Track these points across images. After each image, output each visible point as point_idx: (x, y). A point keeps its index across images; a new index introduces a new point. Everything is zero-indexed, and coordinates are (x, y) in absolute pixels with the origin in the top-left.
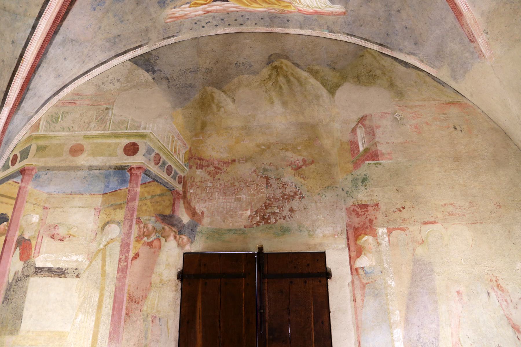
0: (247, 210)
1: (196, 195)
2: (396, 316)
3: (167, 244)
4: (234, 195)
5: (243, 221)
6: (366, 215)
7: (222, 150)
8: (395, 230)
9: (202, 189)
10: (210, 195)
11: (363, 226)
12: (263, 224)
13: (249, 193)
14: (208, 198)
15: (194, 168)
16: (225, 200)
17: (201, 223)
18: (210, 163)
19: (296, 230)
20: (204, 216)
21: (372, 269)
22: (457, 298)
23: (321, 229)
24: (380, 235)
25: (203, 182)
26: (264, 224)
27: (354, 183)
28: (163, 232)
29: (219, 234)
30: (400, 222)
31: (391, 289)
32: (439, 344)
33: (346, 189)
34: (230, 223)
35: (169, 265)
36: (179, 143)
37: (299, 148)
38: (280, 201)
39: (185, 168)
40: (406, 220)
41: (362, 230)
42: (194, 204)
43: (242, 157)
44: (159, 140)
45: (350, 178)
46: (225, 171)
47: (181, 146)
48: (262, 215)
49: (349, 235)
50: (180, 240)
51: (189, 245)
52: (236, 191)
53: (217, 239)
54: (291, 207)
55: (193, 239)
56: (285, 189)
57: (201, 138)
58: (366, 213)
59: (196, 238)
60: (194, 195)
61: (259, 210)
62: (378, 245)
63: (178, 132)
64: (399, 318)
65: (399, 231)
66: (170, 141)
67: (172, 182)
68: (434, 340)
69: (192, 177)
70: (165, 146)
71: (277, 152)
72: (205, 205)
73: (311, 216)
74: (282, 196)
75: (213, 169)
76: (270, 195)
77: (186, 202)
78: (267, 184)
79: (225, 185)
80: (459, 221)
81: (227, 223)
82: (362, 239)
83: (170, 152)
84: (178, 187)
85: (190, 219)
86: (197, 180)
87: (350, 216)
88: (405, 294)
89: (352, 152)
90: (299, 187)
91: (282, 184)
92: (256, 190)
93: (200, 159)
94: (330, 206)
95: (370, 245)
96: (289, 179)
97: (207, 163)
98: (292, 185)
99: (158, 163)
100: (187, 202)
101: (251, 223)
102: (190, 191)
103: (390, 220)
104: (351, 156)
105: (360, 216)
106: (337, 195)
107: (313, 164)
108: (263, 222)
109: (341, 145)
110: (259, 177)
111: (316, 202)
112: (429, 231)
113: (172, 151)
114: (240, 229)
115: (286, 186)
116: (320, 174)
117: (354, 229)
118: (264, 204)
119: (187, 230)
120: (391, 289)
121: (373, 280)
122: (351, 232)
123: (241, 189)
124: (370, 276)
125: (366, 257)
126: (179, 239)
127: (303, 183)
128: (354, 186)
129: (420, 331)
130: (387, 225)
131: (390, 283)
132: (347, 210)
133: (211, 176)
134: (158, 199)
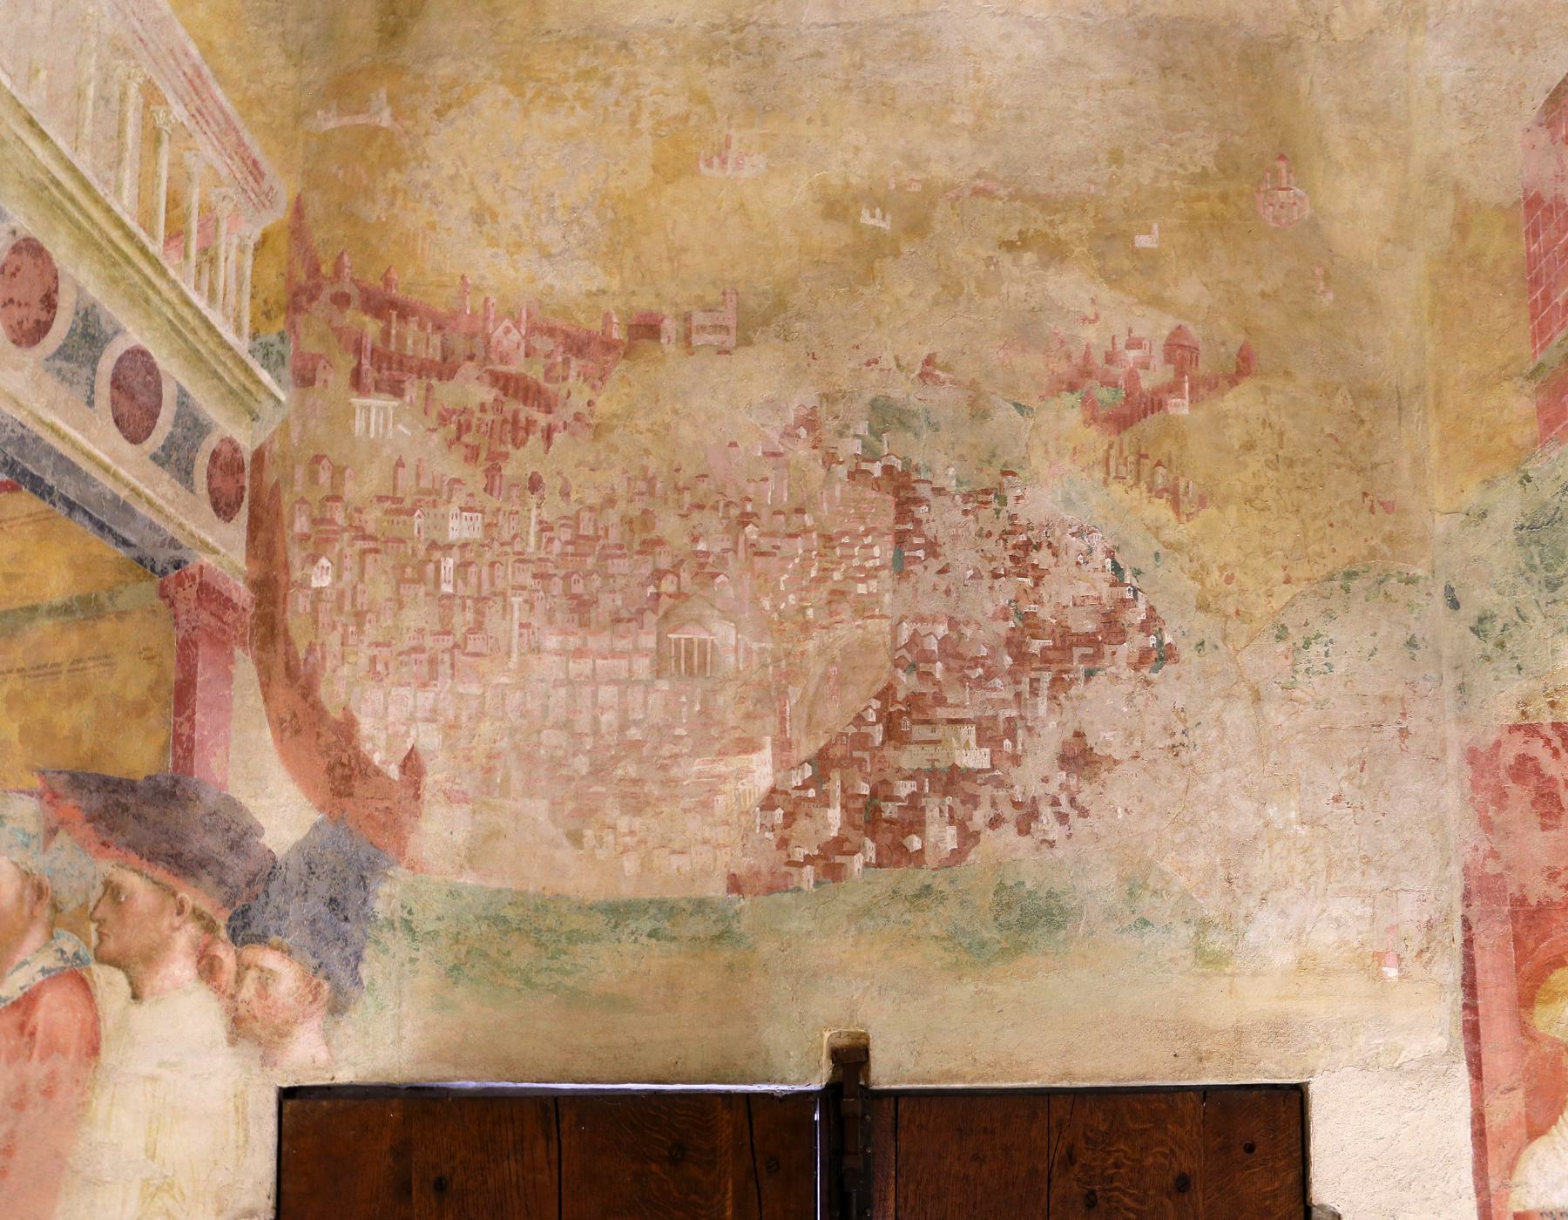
0: (748, 746)
1: (359, 616)
3: (141, 1015)
4: (651, 619)
5: (721, 835)
7: (550, 234)
9: (403, 567)
10: (470, 616)
12: (867, 865)
13: (766, 604)
14: (448, 642)
15: (336, 379)
16: (585, 666)
17: (401, 854)
18: (460, 346)
19: (1111, 915)
20: (426, 795)
23: (1283, 913)
25: (407, 504)
26: (879, 865)
27: (1534, 549)
28: (111, 917)
29: (538, 944)
33: (1480, 597)
34: (626, 850)
35: (167, 1186)
36: (206, 154)
37: (1143, 241)
38: (998, 682)
39: (265, 376)
42: (340, 688)
43: (713, 296)
44: (31, 122)
45: (1509, 506)
46: (578, 417)
47: (219, 183)
48: (865, 789)
49: (1478, 965)
50: (249, 990)
51: (315, 1022)
52: (668, 585)
53: (528, 982)
54: (1079, 735)
55: (343, 976)
56: (1038, 581)
57: (385, 119)
59: (364, 971)
60: (340, 609)
61: (838, 752)
63: (193, 50)
66: (131, 133)
67: (159, 501)
69: (318, 459)
70: (88, 173)
71: (980, 268)
72: (426, 699)
73: (1221, 804)
74: (1009, 642)
75: (487, 394)
76: (923, 629)
77: (279, 671)
78: (901, 539)
79: (577, 539)
81: (601, 854)
83: (130, 236)
84: (210, 540)
85: (318, 817)
86: (364, 484)
87: (1492, 809)
89: (1538, 294)
90: (1137, 573)
91: (1012, 541)
92: (819, 580)
93: (382, 305)
94: (1358, 728)
96: (1068, 502)
97: (436, 340)
98: (1090, 551)
99: (42, 328)
100: (291, 672)
101: (783, 855)
102: (304, 584)
104: (1526, 327)
106: (1411, 643)
107: (1247, 386)
108: (869, 844)
109: (1462, 227)
110: (841, 471)
111: (1257, 698)
113: (147, 223)
114: (701, 905)
115: (1041, 558)
116: (1291, 464)
117: (1514, 915)
118: (876, 704)
119: (297, 910)
122: (1494, 936)
123: (705, 571)
126: (239, 979)
127: (1169, 534)
128: (1535, 577)
132: (1471, 763)
133: (473, 455)
134: (61, 643)
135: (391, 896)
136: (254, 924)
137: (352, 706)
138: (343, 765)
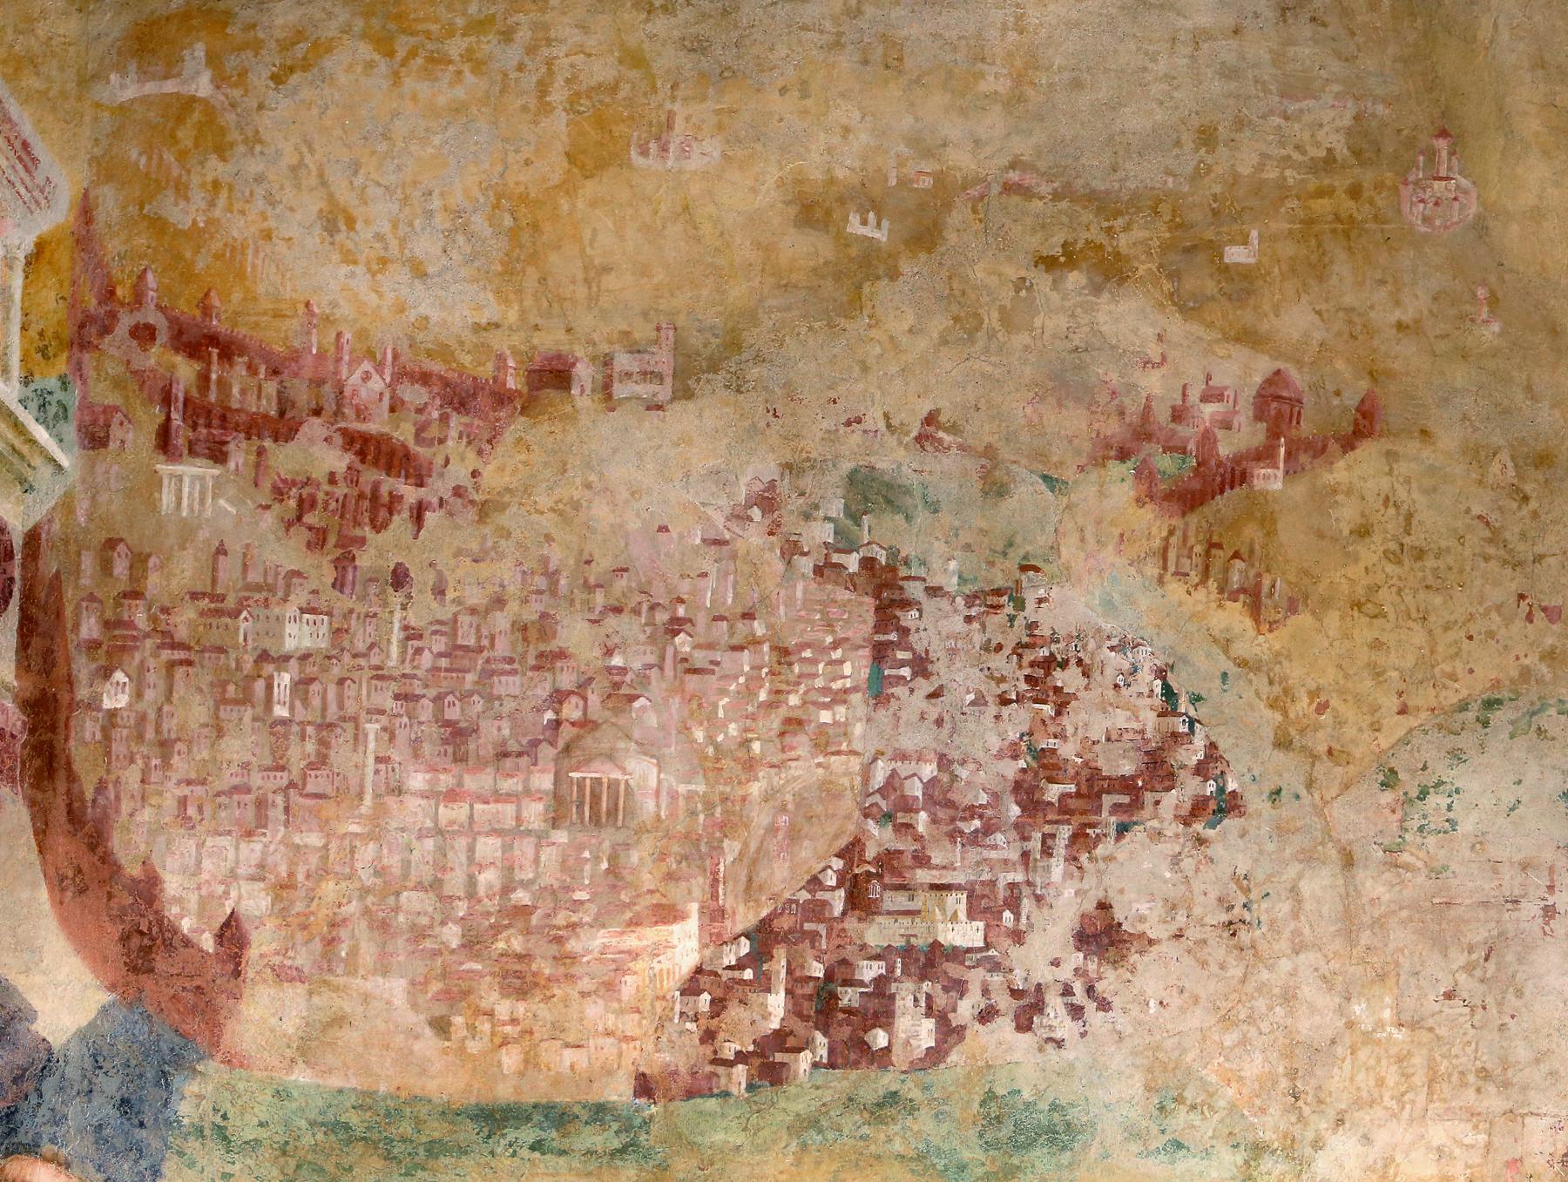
17: (216, 1045)
85: (106, 997)
135: (200, 1097)
136: (22, 1130)
137: (155, 860)
138: (142, 933)
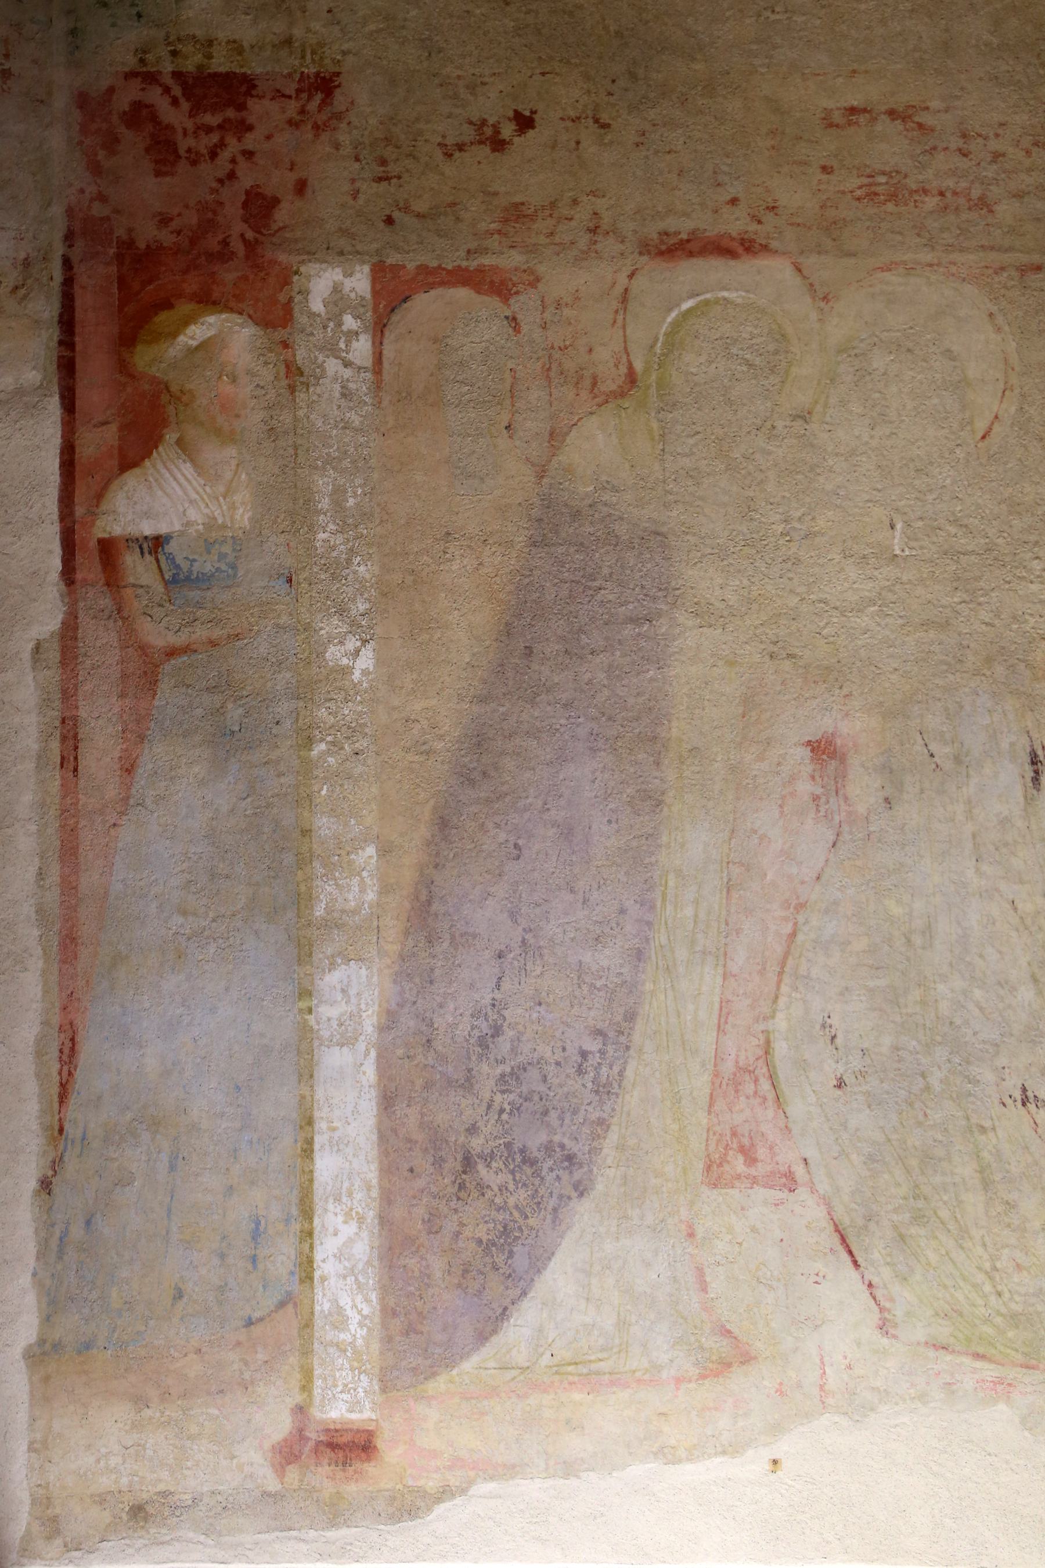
2: (355, 881)
6: (225, 155)
8: (429, 287)
11: (193, 242)
21: (222, 556)
22: (805, 787)
24: (313, 315)
30: (483, 226)
31: (340, 697)
32: (621, 1074)
40: (532, 218)
41: (185, 272)
49: (78, 303)
58: (231, 141)
62: (292, 389)
64: (371, 896)
65: (462, 293)
68: (592, 1045)
80: (931, 245)
82: (174, 335)
87: (101, 154)
88: (441, 737)
95: (234, 380)
103: (406, 209)
105: (183, 166)
112: (689, 311)
117: (120, 257)
120: (340, 697)
121: (217, 633)
124: (199, 605)
125: (188, 469)
129: (506, 985)
130: (375, 246)
131: (345, 661)
132: (81, 107)
